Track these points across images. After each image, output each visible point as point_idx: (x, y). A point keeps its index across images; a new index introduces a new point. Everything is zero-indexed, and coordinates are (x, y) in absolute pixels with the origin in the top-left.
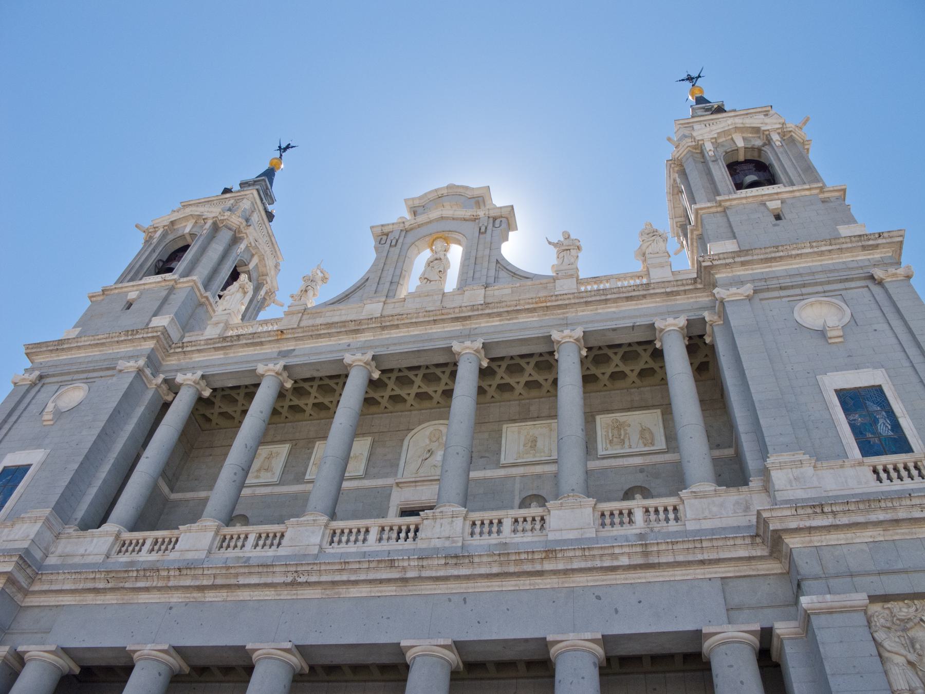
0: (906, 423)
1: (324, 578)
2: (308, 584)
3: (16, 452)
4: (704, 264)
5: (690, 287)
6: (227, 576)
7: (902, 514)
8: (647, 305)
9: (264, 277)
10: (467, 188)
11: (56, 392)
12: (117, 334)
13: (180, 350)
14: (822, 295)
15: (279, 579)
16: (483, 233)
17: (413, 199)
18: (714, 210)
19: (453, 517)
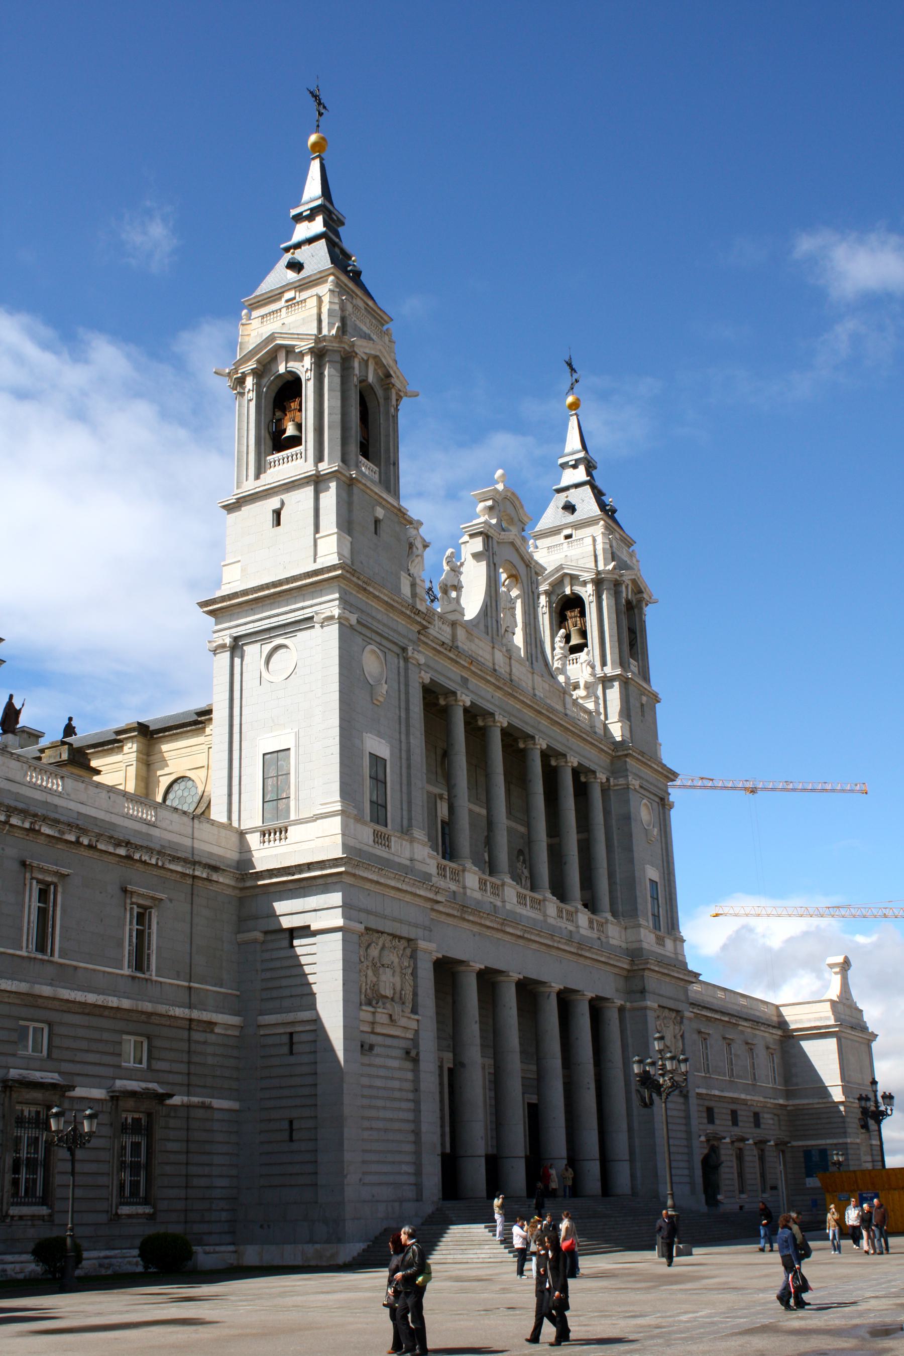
0: (660, 909)
1: (533, 937)
5: (610, 752)
10: (522, 507)
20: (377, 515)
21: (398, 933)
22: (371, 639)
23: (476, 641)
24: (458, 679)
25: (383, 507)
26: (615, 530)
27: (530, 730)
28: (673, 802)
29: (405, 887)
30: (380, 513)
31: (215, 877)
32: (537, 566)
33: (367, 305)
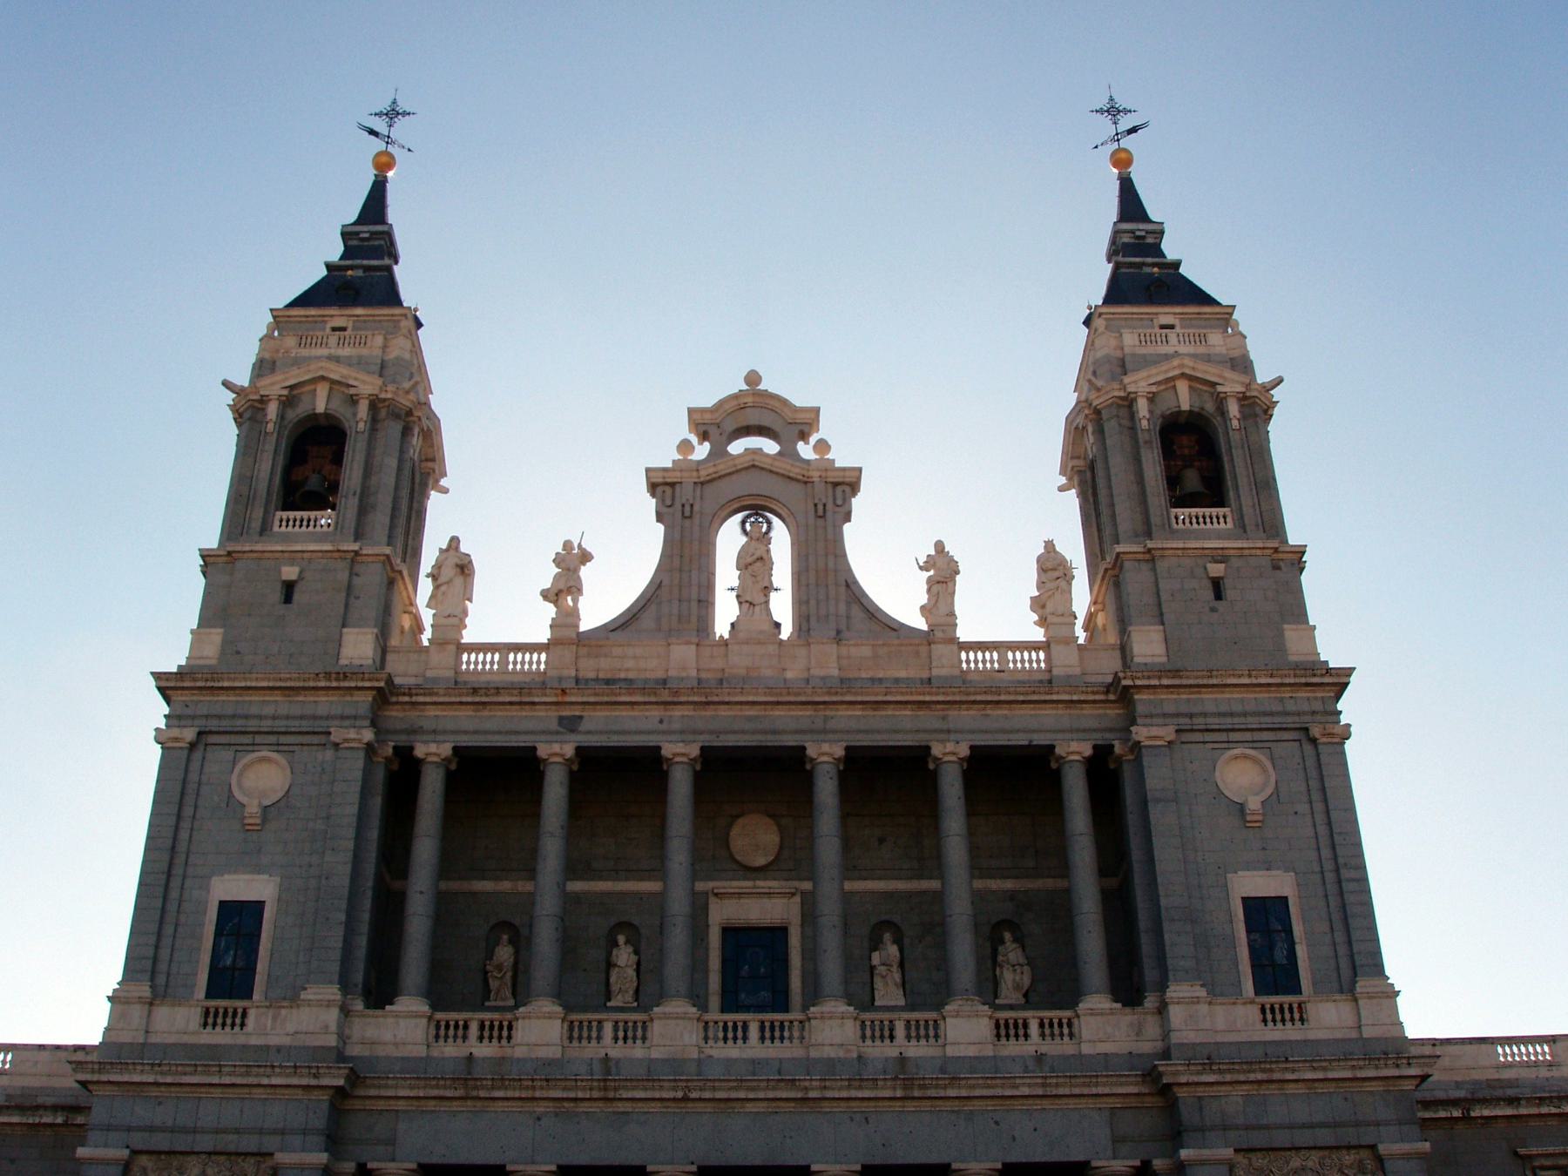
0: (1301, 951)
2: (700, 1099)
3: (226, 877)
4: (1124, 682)
6: (606, 1089)
7: (1276, 1076)
8: (1048, 717)
9: (430, 464)
10: (785, 402)
11: (234, 763)
12: (312, 676)
13: (406, 699)
14: (1246, 745)
15: (671, 1095)
16: (820, 517)
17: (703, 411)
18: (1141, 557)
19: (843, 1018)
20: (284, 578)
21: (232, 1148)
22: (253, 744)
23: (617, 651)
24: (554, 726)
25: (292, 562)
26: (1157, 314)
27: (790, 741)
28: (1349, 726)
29: (227, 1080)
30: (290, 573)
31: (80, 1120)
32: (829, 474)
33: (357, 316)
